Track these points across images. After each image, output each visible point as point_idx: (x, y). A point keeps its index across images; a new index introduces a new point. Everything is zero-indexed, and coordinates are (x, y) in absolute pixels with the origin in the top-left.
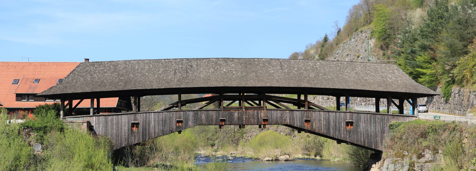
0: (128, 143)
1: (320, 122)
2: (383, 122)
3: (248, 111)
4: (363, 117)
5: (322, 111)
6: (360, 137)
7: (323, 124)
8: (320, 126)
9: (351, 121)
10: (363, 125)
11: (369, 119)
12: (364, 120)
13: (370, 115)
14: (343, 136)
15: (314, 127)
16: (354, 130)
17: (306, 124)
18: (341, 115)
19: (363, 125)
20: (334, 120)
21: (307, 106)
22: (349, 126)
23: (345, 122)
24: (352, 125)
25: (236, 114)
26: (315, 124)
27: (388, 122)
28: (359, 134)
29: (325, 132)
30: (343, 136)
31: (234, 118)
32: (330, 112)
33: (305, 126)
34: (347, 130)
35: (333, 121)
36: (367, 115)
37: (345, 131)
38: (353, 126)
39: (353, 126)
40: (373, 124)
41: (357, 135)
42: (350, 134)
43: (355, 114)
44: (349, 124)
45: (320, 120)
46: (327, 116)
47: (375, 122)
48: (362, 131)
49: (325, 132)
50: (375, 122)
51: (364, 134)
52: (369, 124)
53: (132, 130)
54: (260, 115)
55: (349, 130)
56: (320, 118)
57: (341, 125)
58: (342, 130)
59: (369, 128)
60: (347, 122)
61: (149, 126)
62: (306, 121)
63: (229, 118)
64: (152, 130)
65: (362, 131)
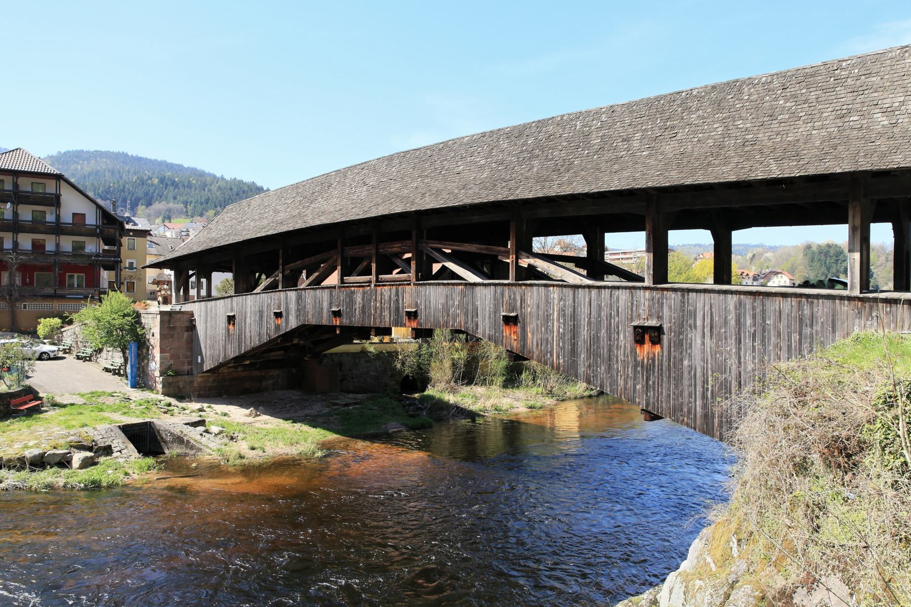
0: (225, 355)
1: (548, 326)
2: (807, 331)
3: (379, 289)
4: (707, 308)
5: (553, 286)
6: (690, 396)
7: (555, 334)
8: (547, 339)
9: (653, 323)
10: (703, 344)
11: (732, 318)
12: (708, 321)
13: (735, 298)
14: (621, 382)
15: (529, 342)
16: (665, 364)
17: (507, 331)
18: (618, 298)
19: (703, 344)
20: (593, 320)
21: (512, 267)
22: (647, 346)
23: (631, 330)
24: (656, 341)
25: (358, 298)
26: (533, 334)
27: (834, 331)
28: (686, 382)
29: (561, 361)
30: (621, 382)
31: (356, 309)
32: (580, 290)
33: (503, 336)
34: (639, 359)
35: (589, 323)
36: (722, 297)
37: (628, 364)
38: (662, 348)
39: (662, 348)
40: (754, 340)
41: (676, 386)
42: (648, 380)
43: (673, 295)
44: (647, 337)
45: (547, 318)
46: (571, 301)
47: (764, 331)
48: (699, 370)
49: (561, 361)
50: (764, 331)
51: (705, 382)
52: (732, 341)
53: (229, 330)
54: (401, 301)
55: (646, 361)
56: (547, 310)
57: (618, 340)
58: (621, 357)
59: (732, 362)
60: (635, 327)
61: (245, 324)
62: (509, 321)
63: (347, 308)
64: (248, 334)
65: (699, 370)
